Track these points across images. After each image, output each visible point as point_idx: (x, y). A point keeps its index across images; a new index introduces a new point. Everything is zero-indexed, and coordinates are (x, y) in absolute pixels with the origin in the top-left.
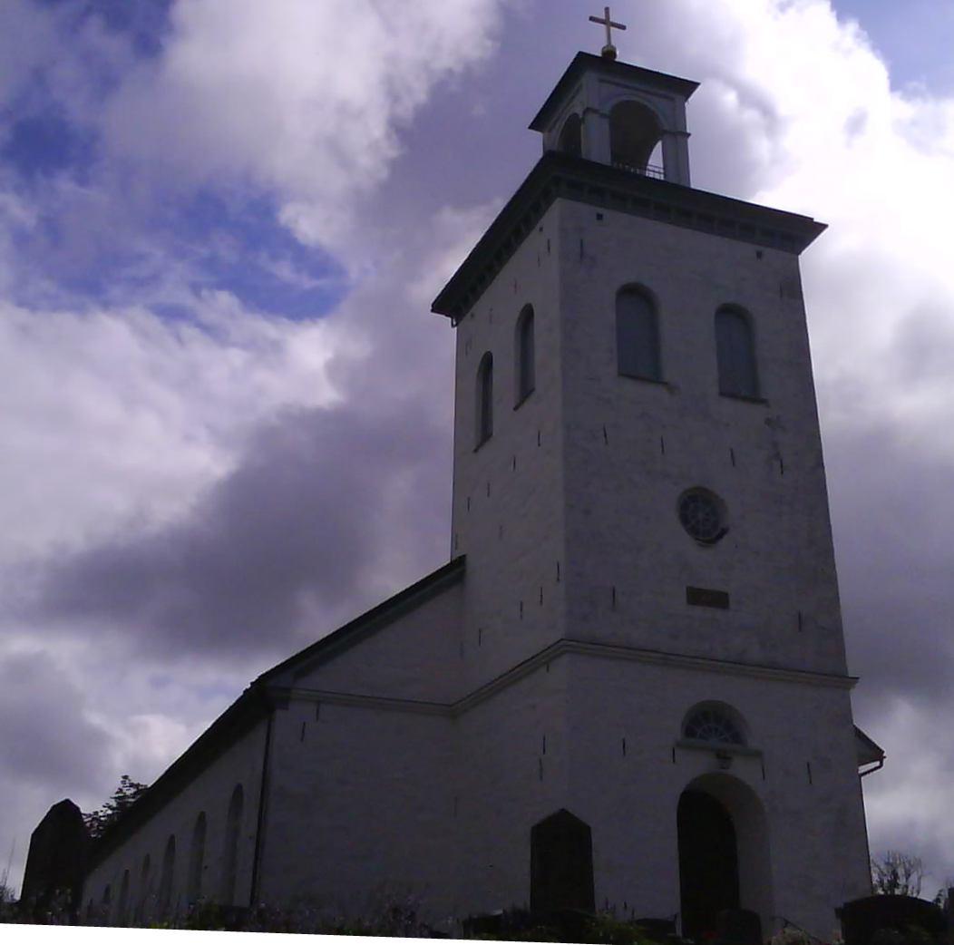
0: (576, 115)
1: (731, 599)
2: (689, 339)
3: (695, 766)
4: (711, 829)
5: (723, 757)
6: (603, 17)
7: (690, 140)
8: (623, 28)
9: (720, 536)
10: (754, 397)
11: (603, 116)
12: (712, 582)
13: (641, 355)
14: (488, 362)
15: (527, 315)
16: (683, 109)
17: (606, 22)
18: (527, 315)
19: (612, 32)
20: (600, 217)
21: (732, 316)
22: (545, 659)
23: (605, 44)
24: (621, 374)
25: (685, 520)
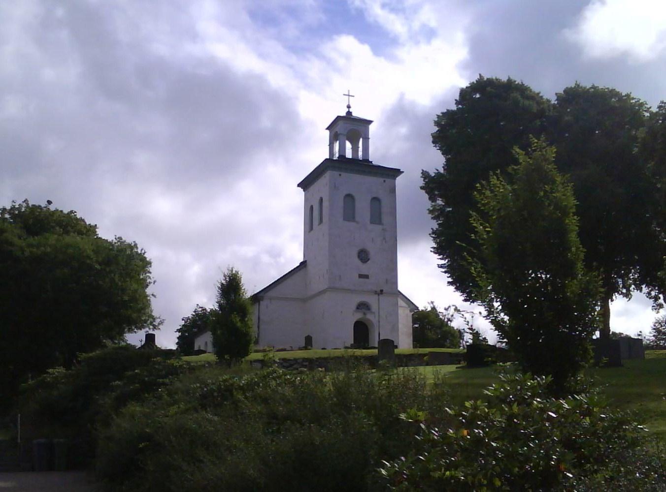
0: (337, 132)
1: (370, 276)
2: (363, 208)
3: (358, 316)
4: (362, 331)
5: (365, 314)
6: (347, 94)
7: (370, 140)
11: (344, 135)
12: (364, 272)
13: (350, 214)
14: (312, 207)
15: (321, 200)
16: (368, 128)
17: (349, 95)
18: (321, 200)
20: (340, 175)
21: (376, 200)
23: (348, 104)
25: (359, 257)
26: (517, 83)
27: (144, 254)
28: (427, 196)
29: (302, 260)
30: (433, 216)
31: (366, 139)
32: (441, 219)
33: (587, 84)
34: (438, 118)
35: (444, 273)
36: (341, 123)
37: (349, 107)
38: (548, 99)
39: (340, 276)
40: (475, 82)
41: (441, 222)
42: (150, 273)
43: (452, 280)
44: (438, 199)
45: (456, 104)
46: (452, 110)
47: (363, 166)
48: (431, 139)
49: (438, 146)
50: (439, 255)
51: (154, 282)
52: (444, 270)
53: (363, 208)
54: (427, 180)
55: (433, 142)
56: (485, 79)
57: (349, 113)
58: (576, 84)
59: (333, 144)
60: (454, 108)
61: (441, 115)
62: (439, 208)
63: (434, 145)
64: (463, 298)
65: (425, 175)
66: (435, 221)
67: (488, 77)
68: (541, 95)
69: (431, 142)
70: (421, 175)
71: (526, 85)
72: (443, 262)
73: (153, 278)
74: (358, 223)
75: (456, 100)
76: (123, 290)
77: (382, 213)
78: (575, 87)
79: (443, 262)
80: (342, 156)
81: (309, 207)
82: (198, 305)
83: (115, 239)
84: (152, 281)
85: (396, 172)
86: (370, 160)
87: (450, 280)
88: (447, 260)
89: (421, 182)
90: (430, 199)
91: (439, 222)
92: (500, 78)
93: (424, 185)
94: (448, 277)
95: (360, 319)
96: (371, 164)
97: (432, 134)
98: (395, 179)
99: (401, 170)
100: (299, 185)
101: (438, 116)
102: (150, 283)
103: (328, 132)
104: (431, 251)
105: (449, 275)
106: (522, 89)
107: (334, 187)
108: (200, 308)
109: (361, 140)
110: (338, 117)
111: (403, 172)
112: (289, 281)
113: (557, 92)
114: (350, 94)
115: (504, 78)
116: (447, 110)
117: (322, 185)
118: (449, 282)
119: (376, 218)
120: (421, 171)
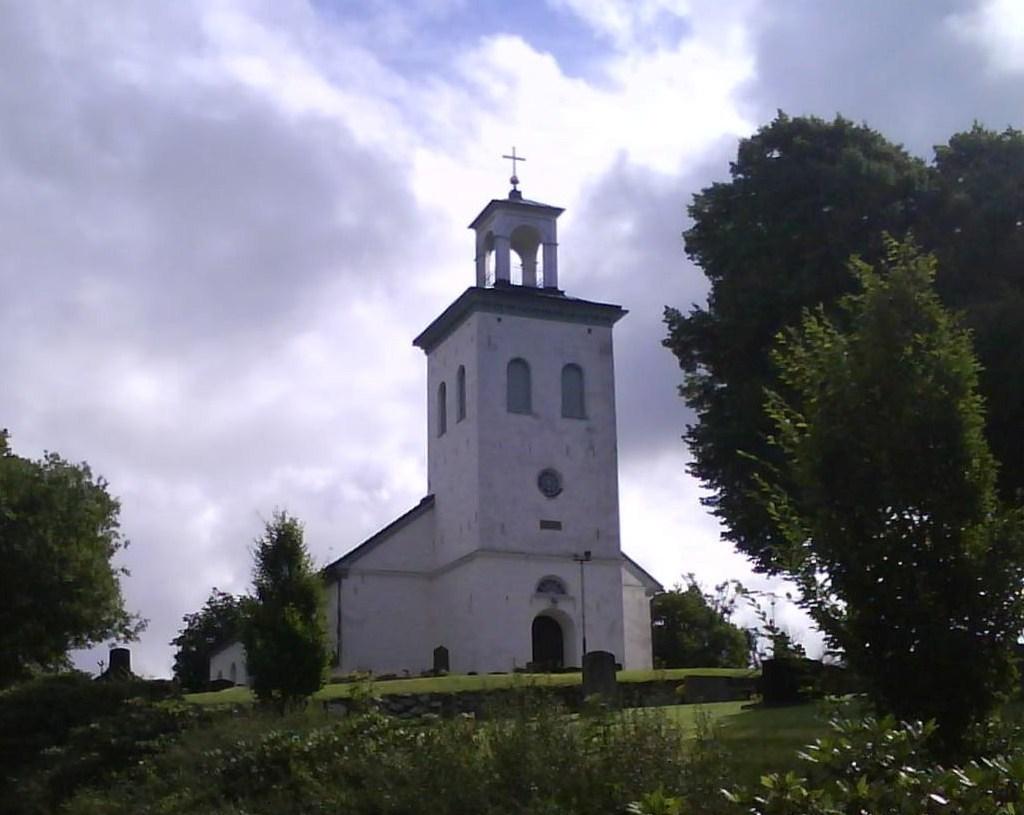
0: (491, 232)
1: (563, 525)
2: (547, 386)
3: (542, 605)
4: (548, 636)
5: (554, 601)
6: (511, 155)
7: (558, 248)
8: (523, 160)
9: (557, 494)
10: (583, 417)
13: (520, 399)
14: (443, 387)
15: (462, 370)
17: (514, 158)
18: (462, 370)
19: (517, 166)
20: (499, 320)
21: (573, 369)
22: (468, 558)
23: (511, 175)
24: (509, 410)
26: (854, 126)
27: (104, 487)
28: (676, 360)
29: (425, 494)
30: (689, 400)
31: (551, 246)
32: (705, 406)
33: (996, 126)
34: (696, 200)
35: (713, 516)
36: (498, 214)
37: (514, 181)
38: (919, 157)
39: (503, 526)
40: (770, 127)
41: (706, 411)
42: (117, 525)
43: (730, 530)
44: (698, 364)
45: (732, 171)
46: (724, 185)
47: (545, 301)
48: (684, 244)
49: (698, 258)
50: (703, 479)
51: (127, 544)
52: (713, 509)
53: (547, 386)
54: (675, 328)
55: (687, 250)
56: (790, 120)
57: (515, 194)
58: (974, 127)
59: (484, 256)
60: (728, 179)
61: (702, 194)
62: (700, 383)
63: (689, 256)
64: (754, 566)
65: (672, 316)
66: (694, 409)
67: (796, 116)
68: (903, 150)
69: (683, 249)
70: (664, 317)
71: (872, 130)
72: (711, 493)
73: (124, 535)
74: (536, 416)
75: (731, 164)
76: (64, 562)
77: (585, 395)
78: (972, 132)
79: (711, 493)
80: (503, 282)
81: (437, 387)
82: (215, 589)
83: (44, 459)
84: (121, 541)
85: (613, 313)
86: (560, 288)
87: (726, 529)
88: (719, 489)
89: (665, 332)
90: (682, 365)
91: (703, 412)
92: (821, 118)
93: (670, 337)
94: (722, 524)
95: (544, 611)
96: (561, 297)
97: (684, 234)
98: (611, 327)
99: (623, 308)
100: (416, 342)
101: (696, 197)
102: (117, 546)
103: (473, 233)
104: (687, 472)
105: (725, 519)
106: (866, 140)
107: (488, 345)
108: (221, 594)
109: (541, 247)
110: (493, 201)
111: (627, 312)
112: (399, 537)
113: (937, 144)
114: (517, 156)
115: (829, 118)
116: (715, 184)
117: (463, 343)
118: (723, 534)
119: (574, 405)
120: (664, 309)
